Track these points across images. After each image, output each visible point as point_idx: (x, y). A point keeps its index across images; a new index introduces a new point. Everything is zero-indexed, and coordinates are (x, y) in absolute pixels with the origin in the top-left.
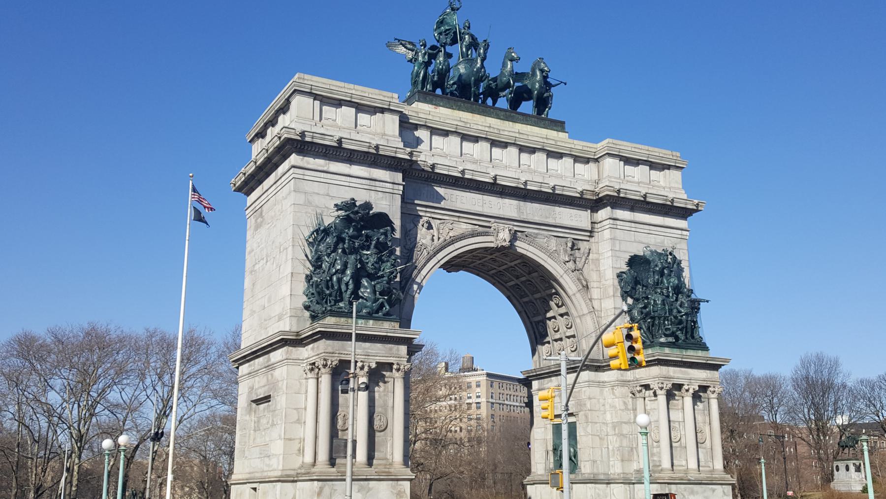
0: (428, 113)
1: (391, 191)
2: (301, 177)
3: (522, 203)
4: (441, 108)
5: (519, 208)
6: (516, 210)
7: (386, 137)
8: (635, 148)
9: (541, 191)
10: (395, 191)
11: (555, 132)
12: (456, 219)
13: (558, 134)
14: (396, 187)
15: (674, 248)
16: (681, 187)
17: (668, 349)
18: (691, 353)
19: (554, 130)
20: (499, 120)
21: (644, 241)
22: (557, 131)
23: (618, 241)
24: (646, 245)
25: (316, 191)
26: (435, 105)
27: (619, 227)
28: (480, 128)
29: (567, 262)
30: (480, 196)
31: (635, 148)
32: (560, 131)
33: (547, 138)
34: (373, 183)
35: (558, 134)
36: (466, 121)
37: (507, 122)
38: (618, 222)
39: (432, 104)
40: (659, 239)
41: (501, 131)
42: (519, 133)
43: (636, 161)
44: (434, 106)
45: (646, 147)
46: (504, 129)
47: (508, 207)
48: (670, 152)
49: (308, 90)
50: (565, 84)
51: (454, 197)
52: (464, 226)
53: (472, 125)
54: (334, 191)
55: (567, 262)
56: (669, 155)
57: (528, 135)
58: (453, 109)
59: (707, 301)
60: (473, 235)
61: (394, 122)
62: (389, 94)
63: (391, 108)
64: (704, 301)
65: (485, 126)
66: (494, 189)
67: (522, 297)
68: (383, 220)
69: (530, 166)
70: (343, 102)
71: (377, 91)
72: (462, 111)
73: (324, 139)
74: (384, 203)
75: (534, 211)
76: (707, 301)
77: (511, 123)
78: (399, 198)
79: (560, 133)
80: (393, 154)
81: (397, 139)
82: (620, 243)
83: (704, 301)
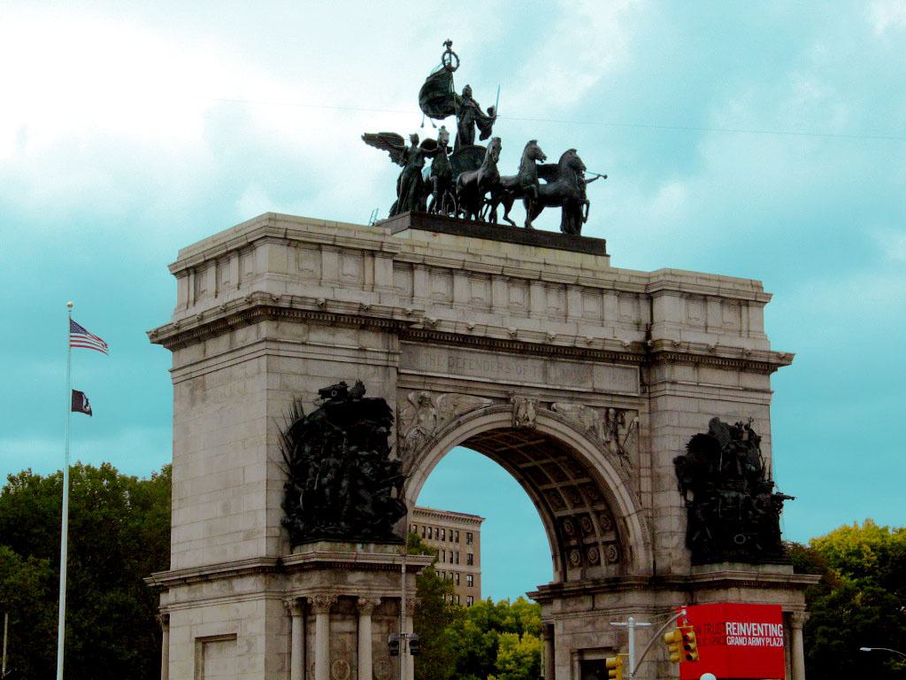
1: (385, 363)
2: (276, 353)
3: (548, 366)
5: (545, 373)
6: (541, 376)
9: (575, 348)
10: (391, 364)
14: (391, 357)
15: (751, 420)
18: (769, 569)
24: (711, 417)
26: (433, 231)
27: (678, 393)
28: (494, 262)
33: (582, 269)
34: (362, 355)
38: (677, 387)
39: (430, 231)
41: (522, 264)
42: (545, 264)
43: (702, 297)
47: (528, 373)
50: (605, 177)
52: (472, 400)
53: (483, 258)
54: (314, 367)
59: (793, 498)
63: (385, 250)
64: (789, 498)
66: (517, 348)
67: (542, 483)
69: (558, 309)
70: (323, 247)
72: (469, 236)
73: (305, 303)
74: (376, 379)
75: (561, 375)
76: (793, 498)
77: (533, 248)
80: (388, 316)
82: (679, 416)
83: (789, 498)
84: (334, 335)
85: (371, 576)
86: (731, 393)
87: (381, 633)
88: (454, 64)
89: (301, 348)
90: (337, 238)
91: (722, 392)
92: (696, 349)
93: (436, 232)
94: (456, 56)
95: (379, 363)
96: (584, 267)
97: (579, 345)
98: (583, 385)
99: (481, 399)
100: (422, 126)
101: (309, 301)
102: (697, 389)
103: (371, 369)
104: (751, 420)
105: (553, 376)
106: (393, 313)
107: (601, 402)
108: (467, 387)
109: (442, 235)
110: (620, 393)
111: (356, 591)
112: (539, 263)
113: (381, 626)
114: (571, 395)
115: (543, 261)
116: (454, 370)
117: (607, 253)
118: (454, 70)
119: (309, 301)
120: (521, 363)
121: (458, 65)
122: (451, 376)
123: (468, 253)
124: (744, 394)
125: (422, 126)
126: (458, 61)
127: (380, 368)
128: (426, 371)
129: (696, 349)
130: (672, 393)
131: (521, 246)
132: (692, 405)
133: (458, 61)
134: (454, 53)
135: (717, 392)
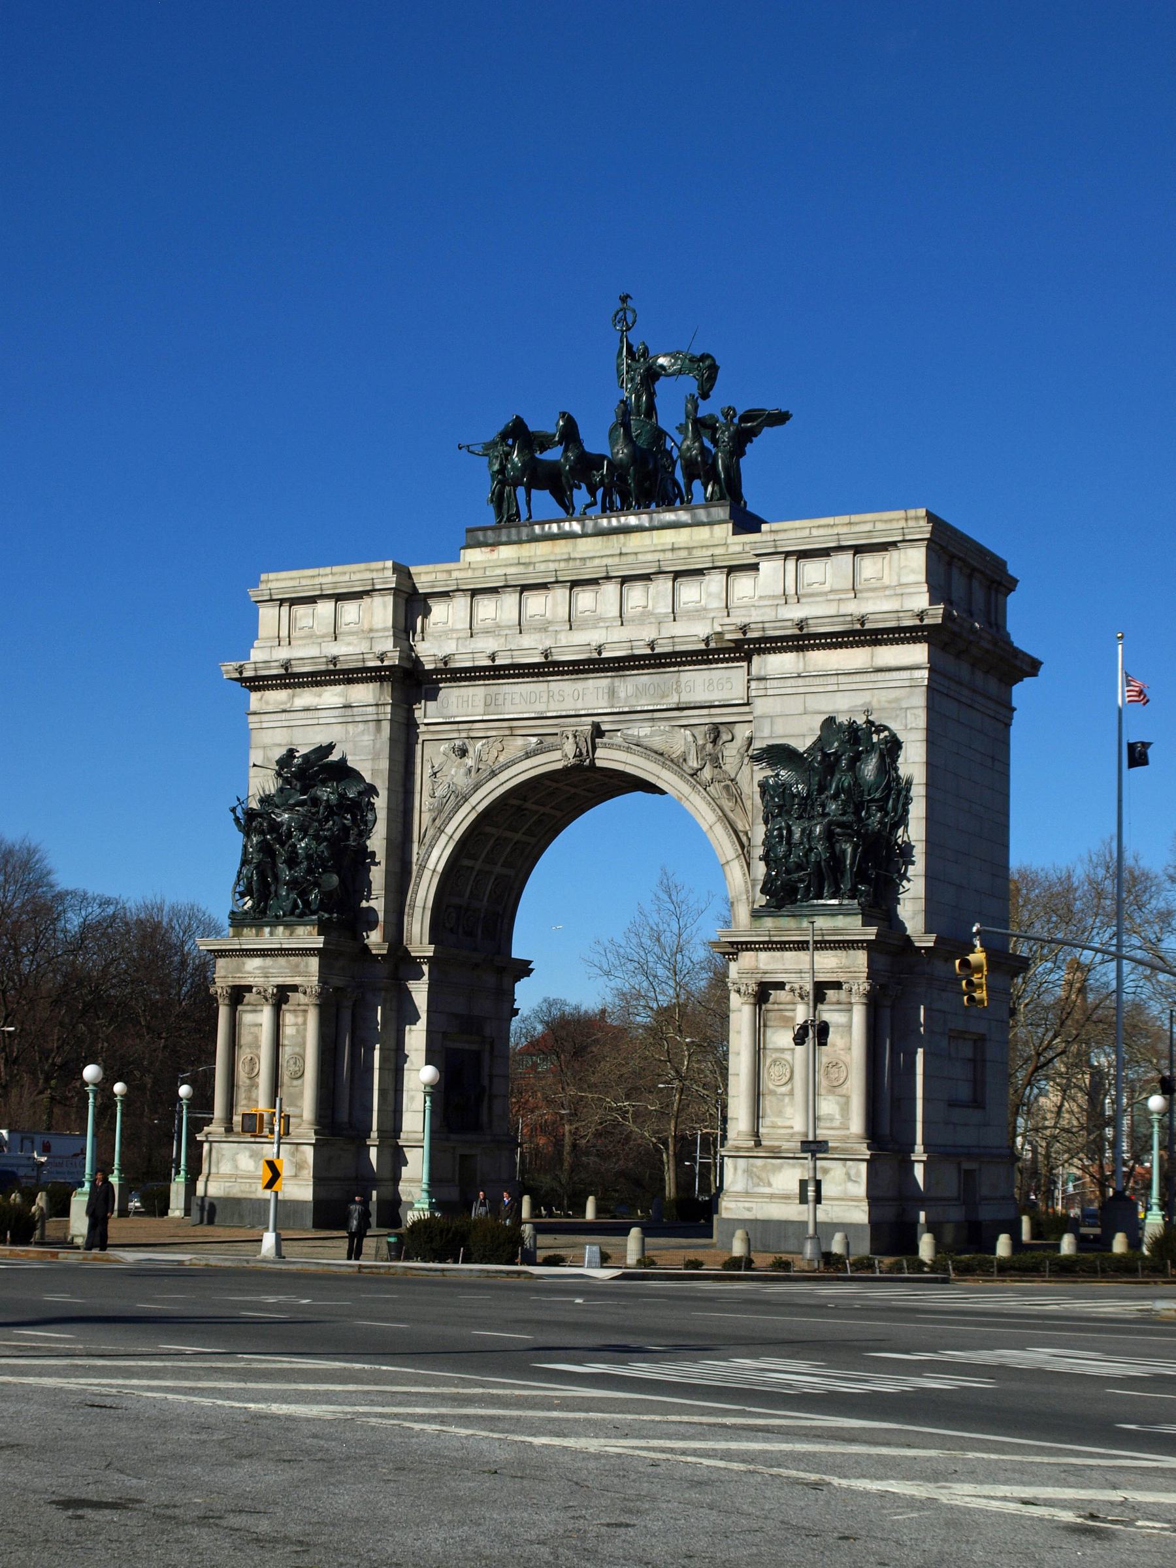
0: (467, 566)
1: (375, 717)
5: (612, 693)
6: (606, 697)
7: (372, 635)
8: (819, 527)
11: (707, 528)
12: (507, 732)
16: (923, 578)
17: (769, 919)
20: (600, 538)
21: (824, 708)
23: (769, 719)
24: (826, 716)
25: (279, 742)
27: (770, 692)
29: (701, 769)
30: (542, 687)
31: (819, 527)
33: (673, 549)
34: (349, 712)
36: (527, 560)
37: (615, 536)
38: (769, 684)
40: (860, 700)
42: (621, 554)
45: (845, 519)
46: (591, 555)
48: (900, 514)
49: (267, 598)
51: (501, 698)
52: (520, 741)
55: (701, 769)
56: (898, 520)
57: (636, 554)
60: (528, 755)
61: (385, 606)
62: (380, 565)
63: (378, 587)
65: (559, 561)
68: (343, 772)
71: (362, 566)
73: (269, 668)
74: (366, 738)
77: (621, 536)
78: (386, 727)
80: (360, 665)
81: (387, 634)
84: (320, 696)
85: (269, 961)
86: (857, 678)
87: (296, 1024)
89: (284, 716)
90: (323, 586)
91: (842, 679)
92: (775, 629)
94: (634, 311)
95: (370, 718)
96: (675, 546)
97: (637, 652)
98: (664, 701)
99: (529, 738)
101: (273, 664)
102: (800, 681)
103: (361, 726)
104: (867, 712)
105: (622, 695)
106: (364, 660)
107: (694, 718)
108: (512, 727)
109: (502, 548)
110: (717, 703)
111: (252, 979)
112: (612, 555)
113: (296, 1016)
114: (649, 715)
115: (618, 552)
116: (492, 708)
119: (273, 664)
120: (580, 685)
122: (485, 718)
123: (519, 564)
124: (880, 676)
127: (371, 724)
128: (454, 717)
129: (775, 629)
130: (762, 692)
131: (605, 537)
132: (795, 705)
135: (834, 680)
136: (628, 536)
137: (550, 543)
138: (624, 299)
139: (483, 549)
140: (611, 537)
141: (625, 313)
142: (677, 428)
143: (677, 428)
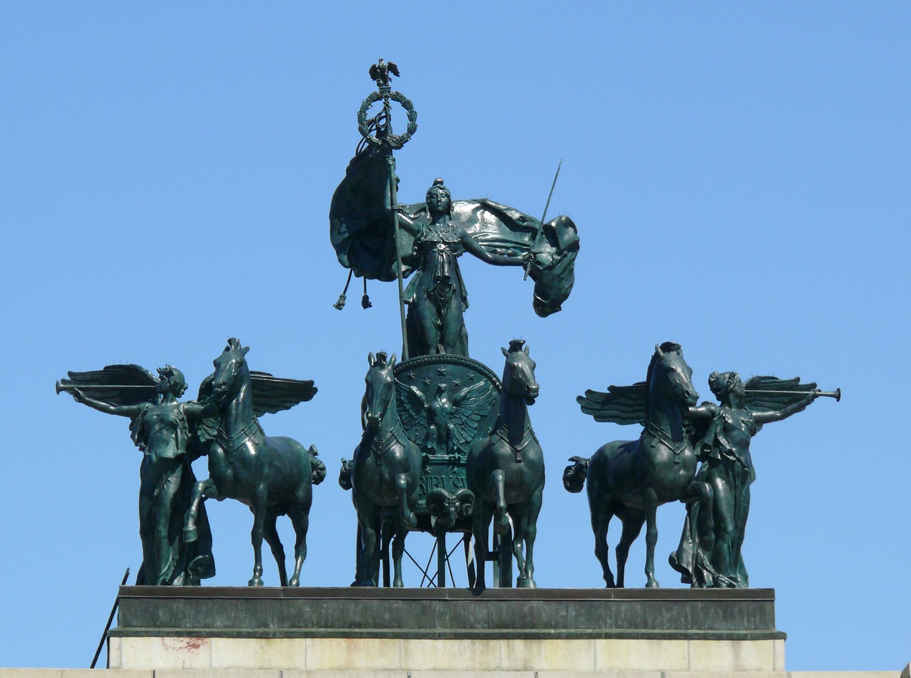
4: (214, 640)
11: (725, 645)
13: (737, 656)
19: (719, 638)
20: (467, 642)
22: (730, 637)
26: (190, 634)
32: (744, 638)
35: (737, 656)
37: (503, 643)
39: (179, 635)
44: (187, 640)
50: (837, 396)
58: (265, 636)
77: (519, 644)
79: (747, 645)
88: (399, 125)
93: (199, 635)
94: (407, 105)
100: (339, 306)
117: (779, 627)
118: (401, 143)
121: (412, 130)
125: (339, 306)
126: (412, 117)
131: (478, 643)
133: (412, 117)
134: (397, 98)
136: (535, 644)
137: (343, 642)
138: (379, 73)
139: (168, 640)
140: (492, 643)
141: (387, 108)
142: (579, 399)
143: (579, 399)
